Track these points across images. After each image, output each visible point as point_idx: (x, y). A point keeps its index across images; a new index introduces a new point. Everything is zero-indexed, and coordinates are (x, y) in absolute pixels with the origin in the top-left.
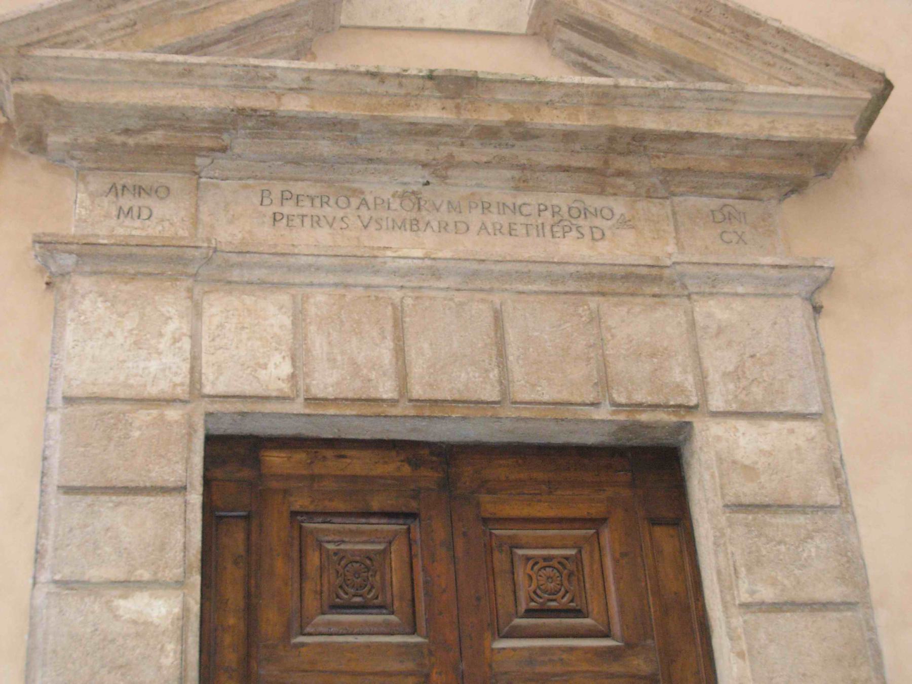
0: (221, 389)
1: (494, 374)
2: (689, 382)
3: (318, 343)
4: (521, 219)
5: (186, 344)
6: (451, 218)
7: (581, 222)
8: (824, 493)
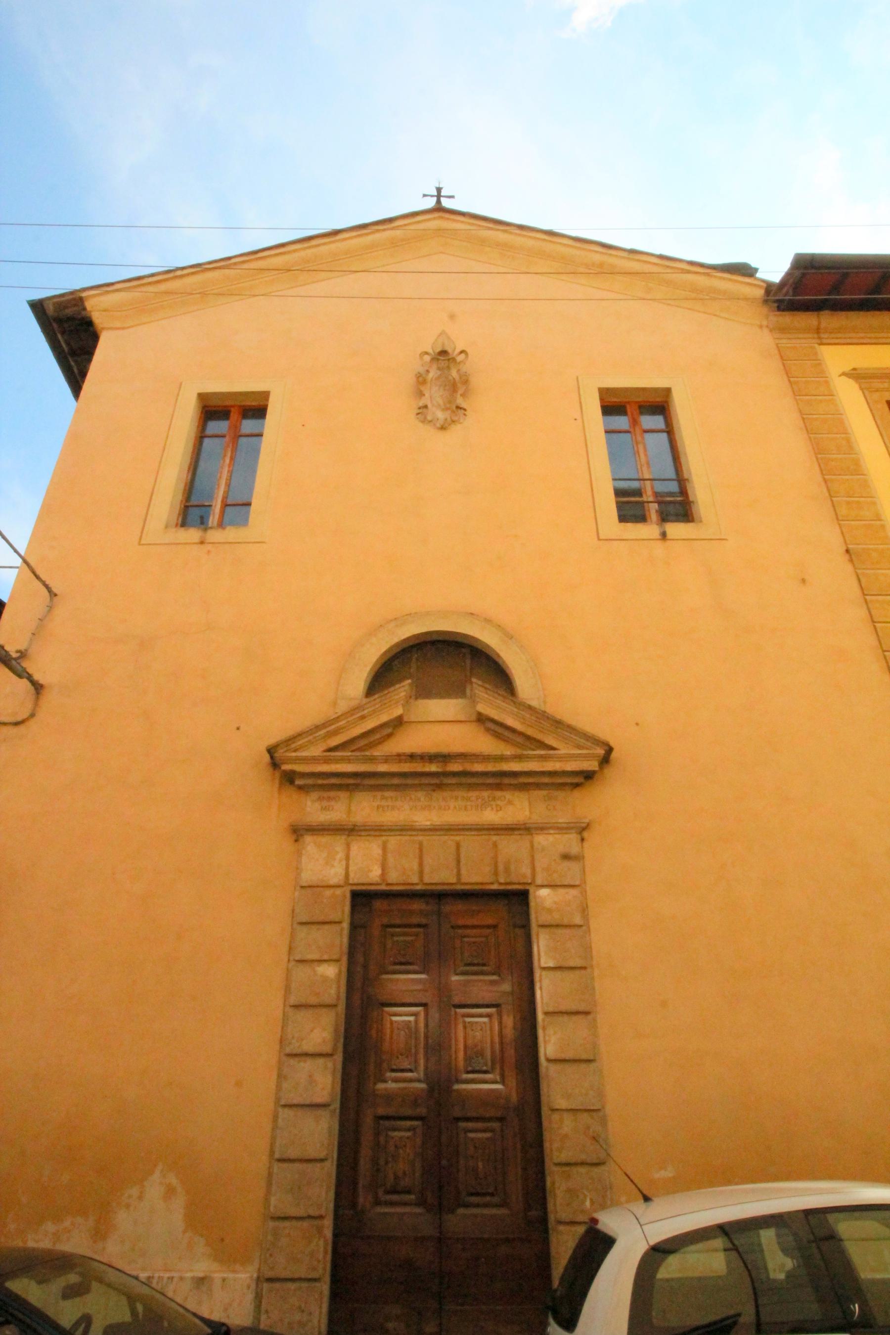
0: (356, 881)
1: (455, 871)
2: (528, 872)
3: (391, 860)
4: (469, 803)
5: (344, 863)
6: (443, 804)
7: (492, 803)
8: (578, 920)
